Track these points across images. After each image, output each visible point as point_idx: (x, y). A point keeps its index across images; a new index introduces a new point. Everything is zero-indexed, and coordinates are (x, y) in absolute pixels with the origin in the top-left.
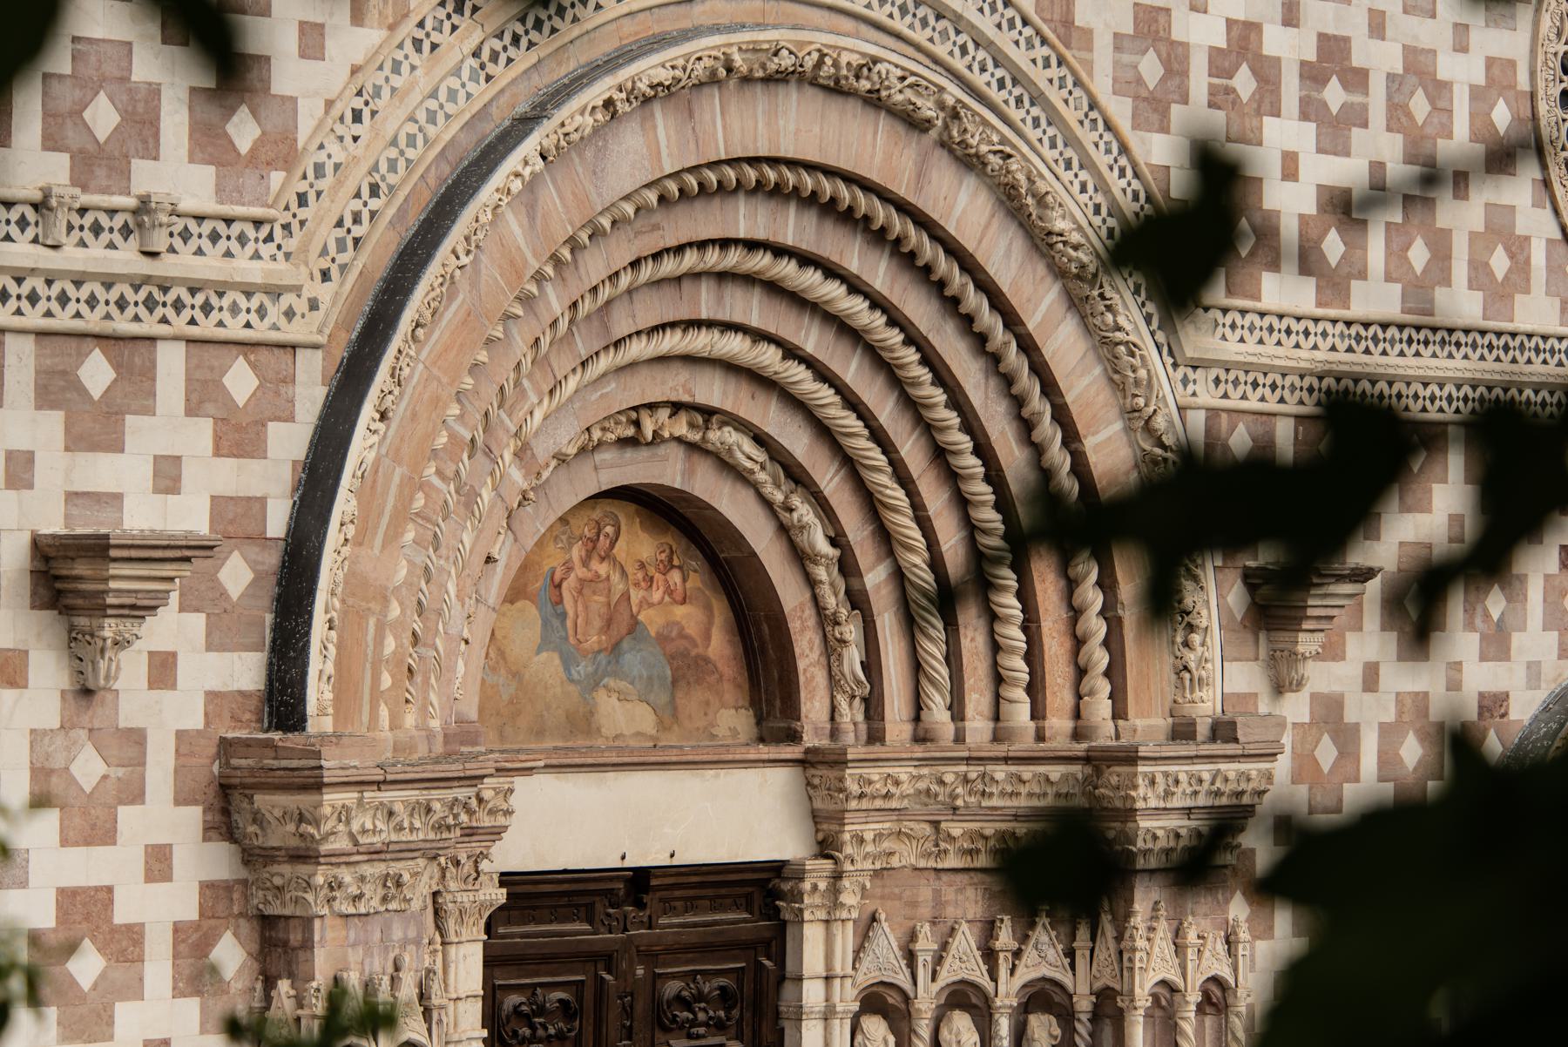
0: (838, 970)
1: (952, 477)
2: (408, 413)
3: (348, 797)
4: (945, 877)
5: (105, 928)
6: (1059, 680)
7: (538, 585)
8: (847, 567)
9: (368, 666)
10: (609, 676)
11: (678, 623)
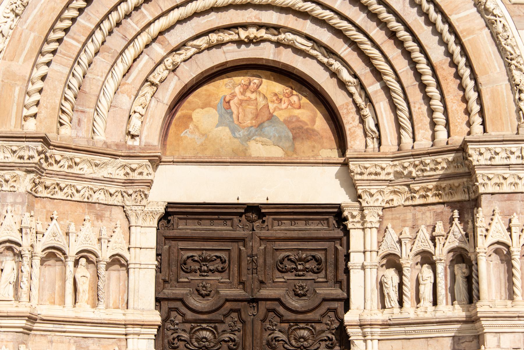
0: (368, 248)
1: (400, 43)
2: (39, 13)
4: (417, 208)
6: (458, 120)
7: (217, 102)
9: (15, 104)
10: (256, 135)
11: (296, 116)
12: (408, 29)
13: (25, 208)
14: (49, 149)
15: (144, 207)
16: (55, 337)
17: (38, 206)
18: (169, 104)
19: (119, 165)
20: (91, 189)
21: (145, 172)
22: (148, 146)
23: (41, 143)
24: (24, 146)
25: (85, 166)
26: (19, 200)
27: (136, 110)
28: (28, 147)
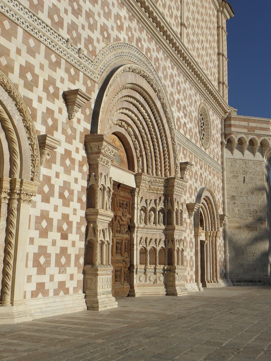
8: (141, 152)
12: (157, 139)
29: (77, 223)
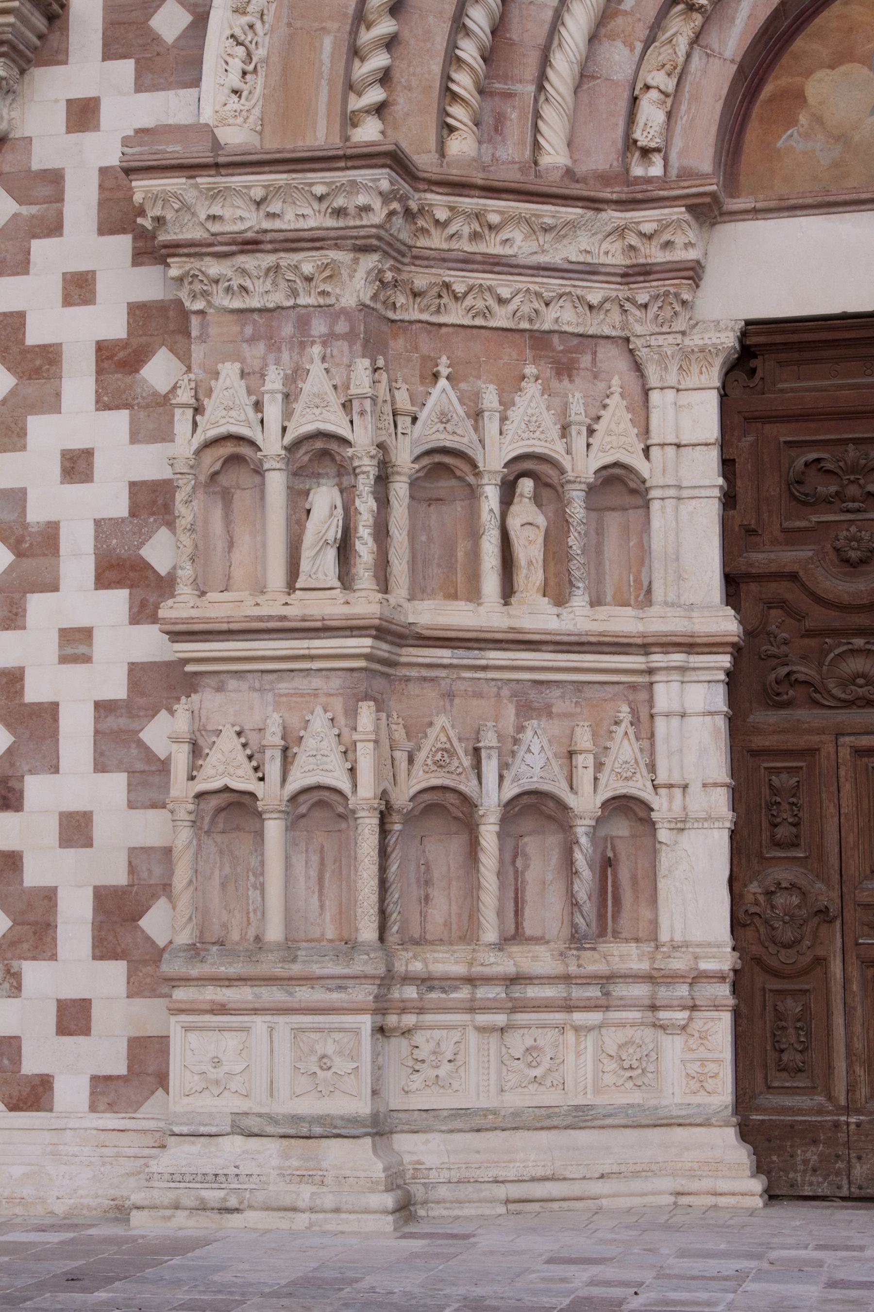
3: (174, 183)
5: (14, 349)
9: (324, 83)
13: (358, 347)
14: (417, 190)
15: (679, 336)
16: (459, 682)
17: (398, 345)
18: (738, 59)
19: (609, 228)
20: (538, 295)
21: (679, 240)
22: (686, 174)
23: (387, 170)
24: (344, 180)
25: (517, 235)
26: (342, 327)
27: (651, 82)
28: (353, 183)
29: (103, 708)
